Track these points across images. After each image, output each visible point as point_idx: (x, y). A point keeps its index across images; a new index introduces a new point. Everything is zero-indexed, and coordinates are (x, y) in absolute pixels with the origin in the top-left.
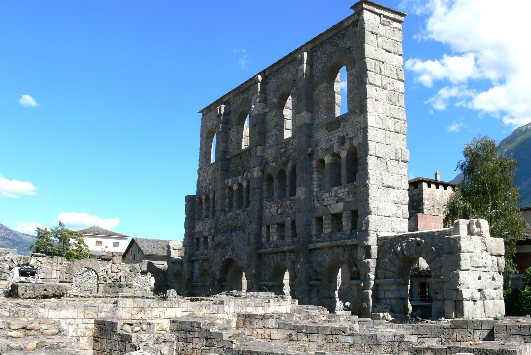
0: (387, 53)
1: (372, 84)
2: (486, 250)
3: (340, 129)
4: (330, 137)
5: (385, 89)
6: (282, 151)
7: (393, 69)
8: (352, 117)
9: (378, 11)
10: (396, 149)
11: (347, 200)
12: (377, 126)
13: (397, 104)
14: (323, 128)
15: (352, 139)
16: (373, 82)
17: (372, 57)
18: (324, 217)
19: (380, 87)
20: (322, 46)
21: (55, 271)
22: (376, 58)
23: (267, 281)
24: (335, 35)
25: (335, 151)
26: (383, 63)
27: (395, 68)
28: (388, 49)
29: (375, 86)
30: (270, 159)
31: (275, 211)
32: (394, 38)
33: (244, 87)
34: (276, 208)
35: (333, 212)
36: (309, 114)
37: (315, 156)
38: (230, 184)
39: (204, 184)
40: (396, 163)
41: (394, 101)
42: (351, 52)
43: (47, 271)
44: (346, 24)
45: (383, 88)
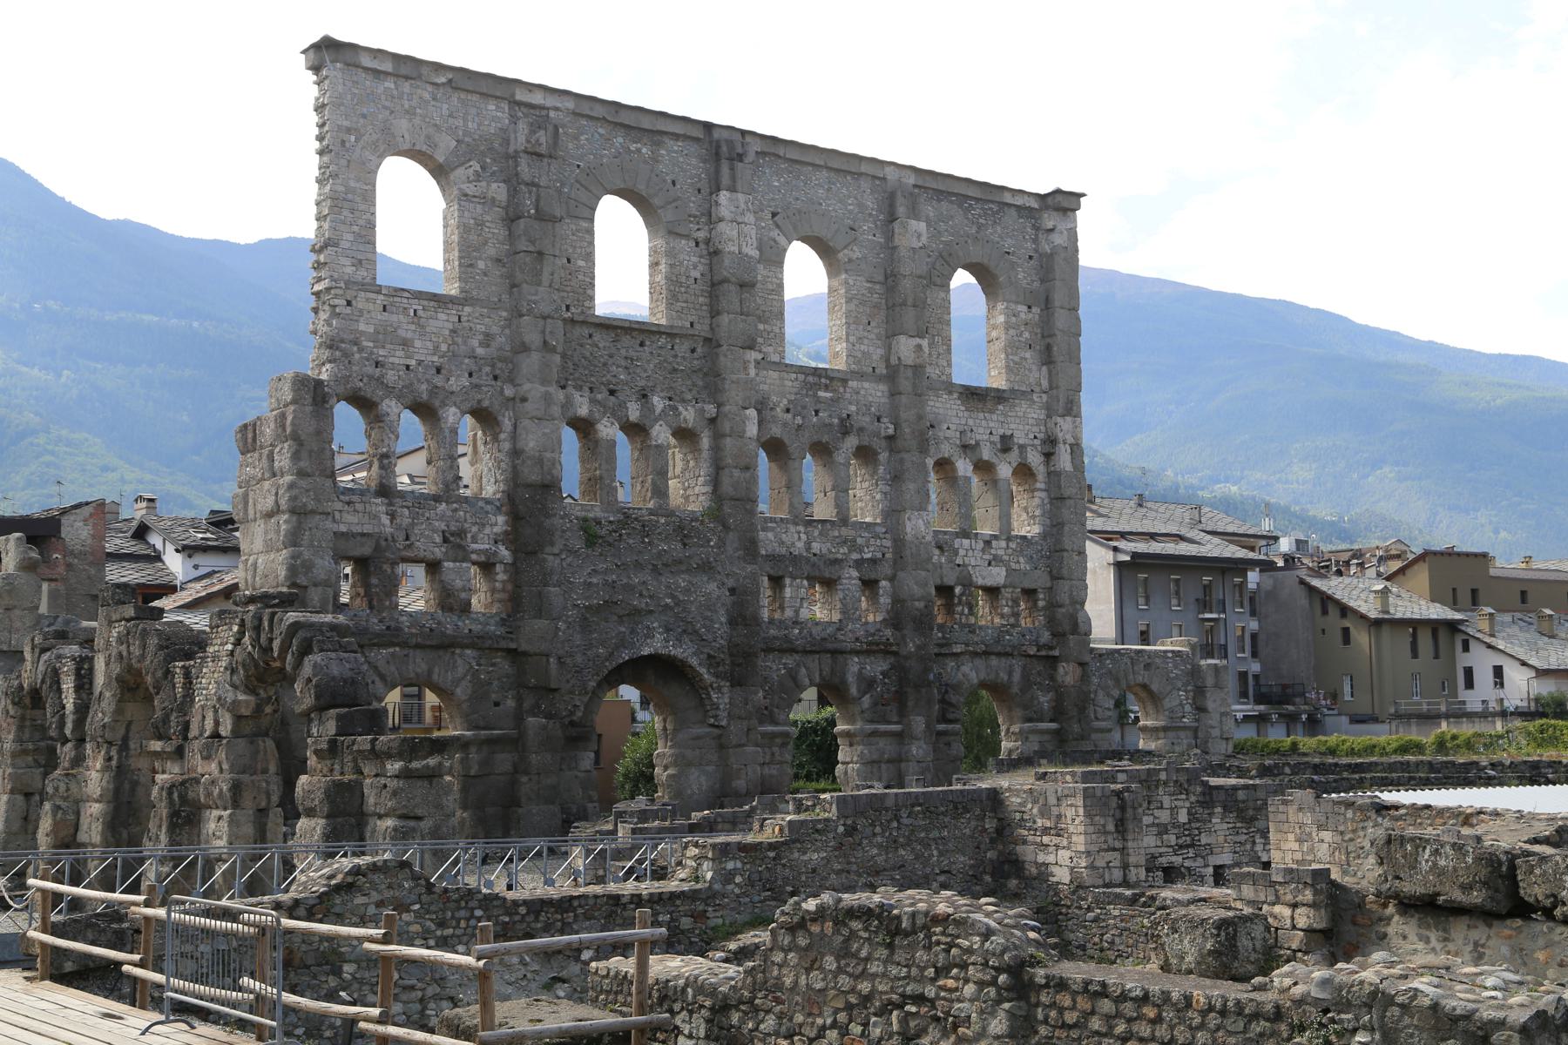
3: (994, 417)
4: (971, 422)
6: (821, 394)
8: (1024, 404)
11: (1013, 566)
14: (950, 393)
15: (1022, 447)
18: (958, 590)
20: (939, 201)
23: (777, 724)
24: (977, 200)
25: (985, 457)
30: (774, 399)
31: (800, 545)
33: (646, 123)
34: (803, 537)
35: (980, 582)
37: (932, 450)
38: (583, 411)
39: (398, 358)
42: (1013, 265)
44: (1008, 198)
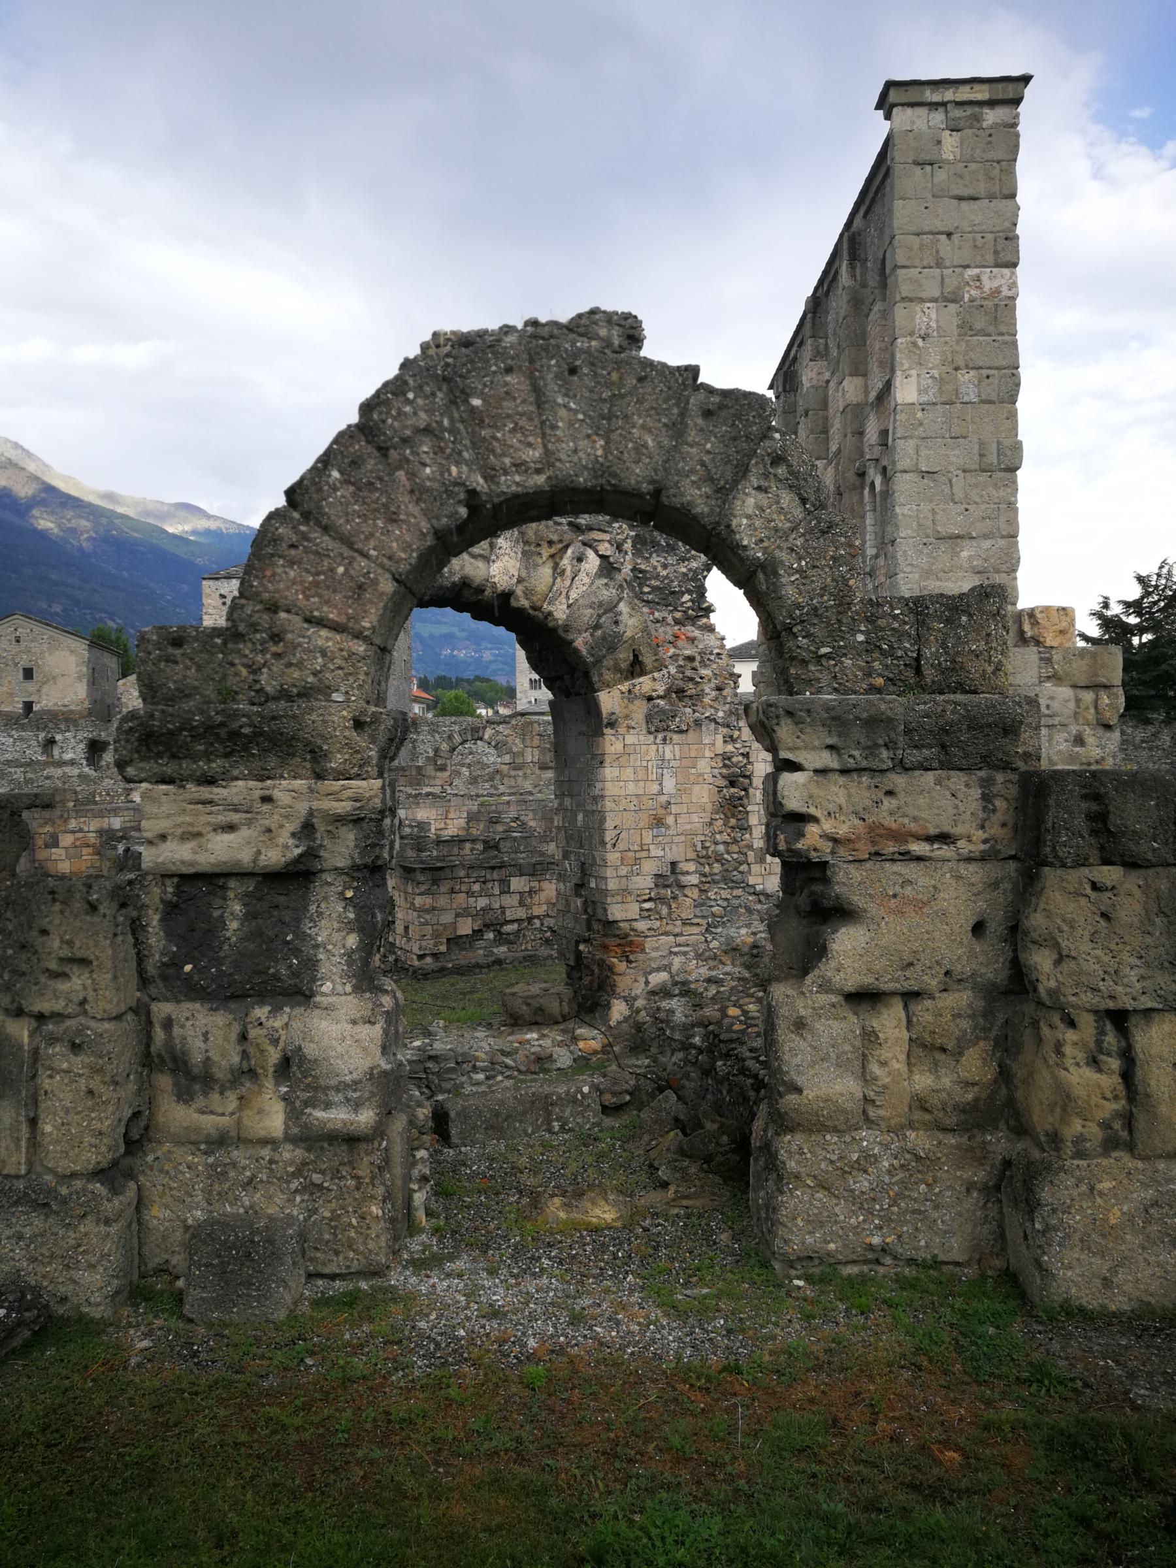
0: (965, 205)
1: (911, 300)
2: (1056, 678)
5: (954, 301)
7: (979, 242)
9: (936, 98)
10: (981, 443)
12: (925, 399)
13: (991, 329)
16: (911, 295)
17: (913, 229)
19: (934, 300)
21: (530, 749)
22: (927, 229)
26: (949, 235)
27: (990, 237)
28: (965, 192)
29: (922, 300)
32: (991, 155)
36: (858, 381)
40: (983, 477)
41: (978, 326)
43: (515, 749)
45: (946, 300)
